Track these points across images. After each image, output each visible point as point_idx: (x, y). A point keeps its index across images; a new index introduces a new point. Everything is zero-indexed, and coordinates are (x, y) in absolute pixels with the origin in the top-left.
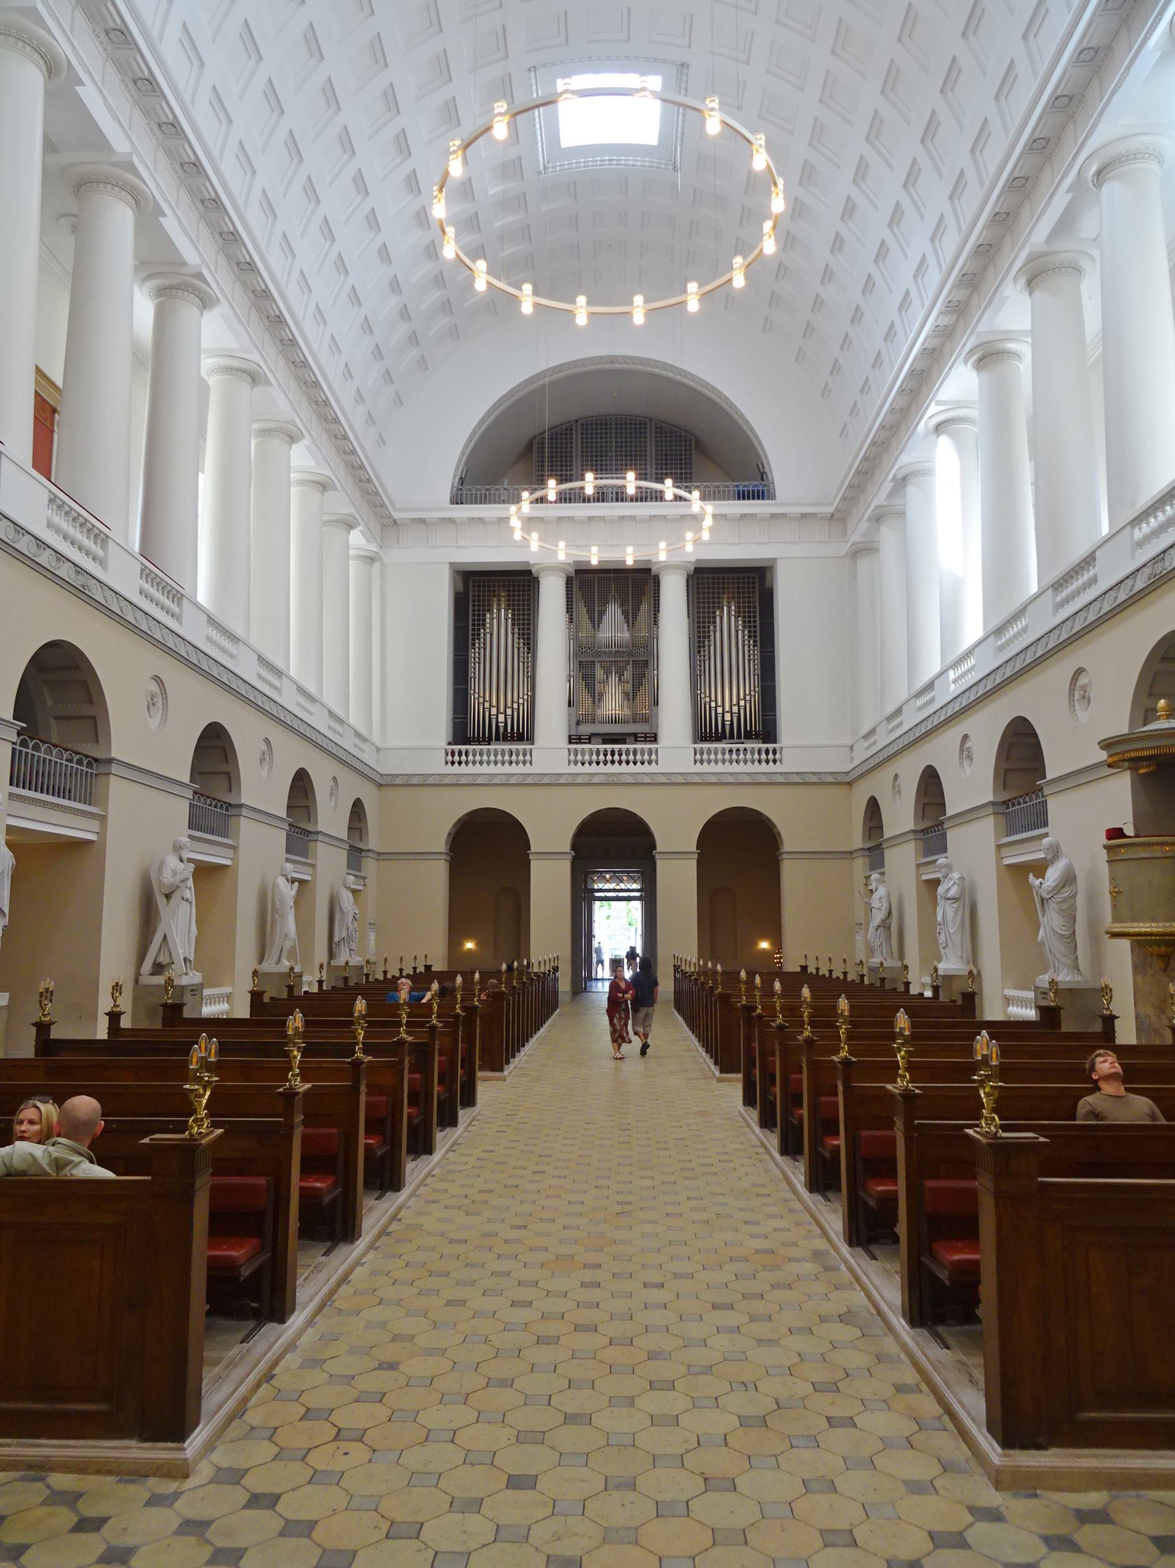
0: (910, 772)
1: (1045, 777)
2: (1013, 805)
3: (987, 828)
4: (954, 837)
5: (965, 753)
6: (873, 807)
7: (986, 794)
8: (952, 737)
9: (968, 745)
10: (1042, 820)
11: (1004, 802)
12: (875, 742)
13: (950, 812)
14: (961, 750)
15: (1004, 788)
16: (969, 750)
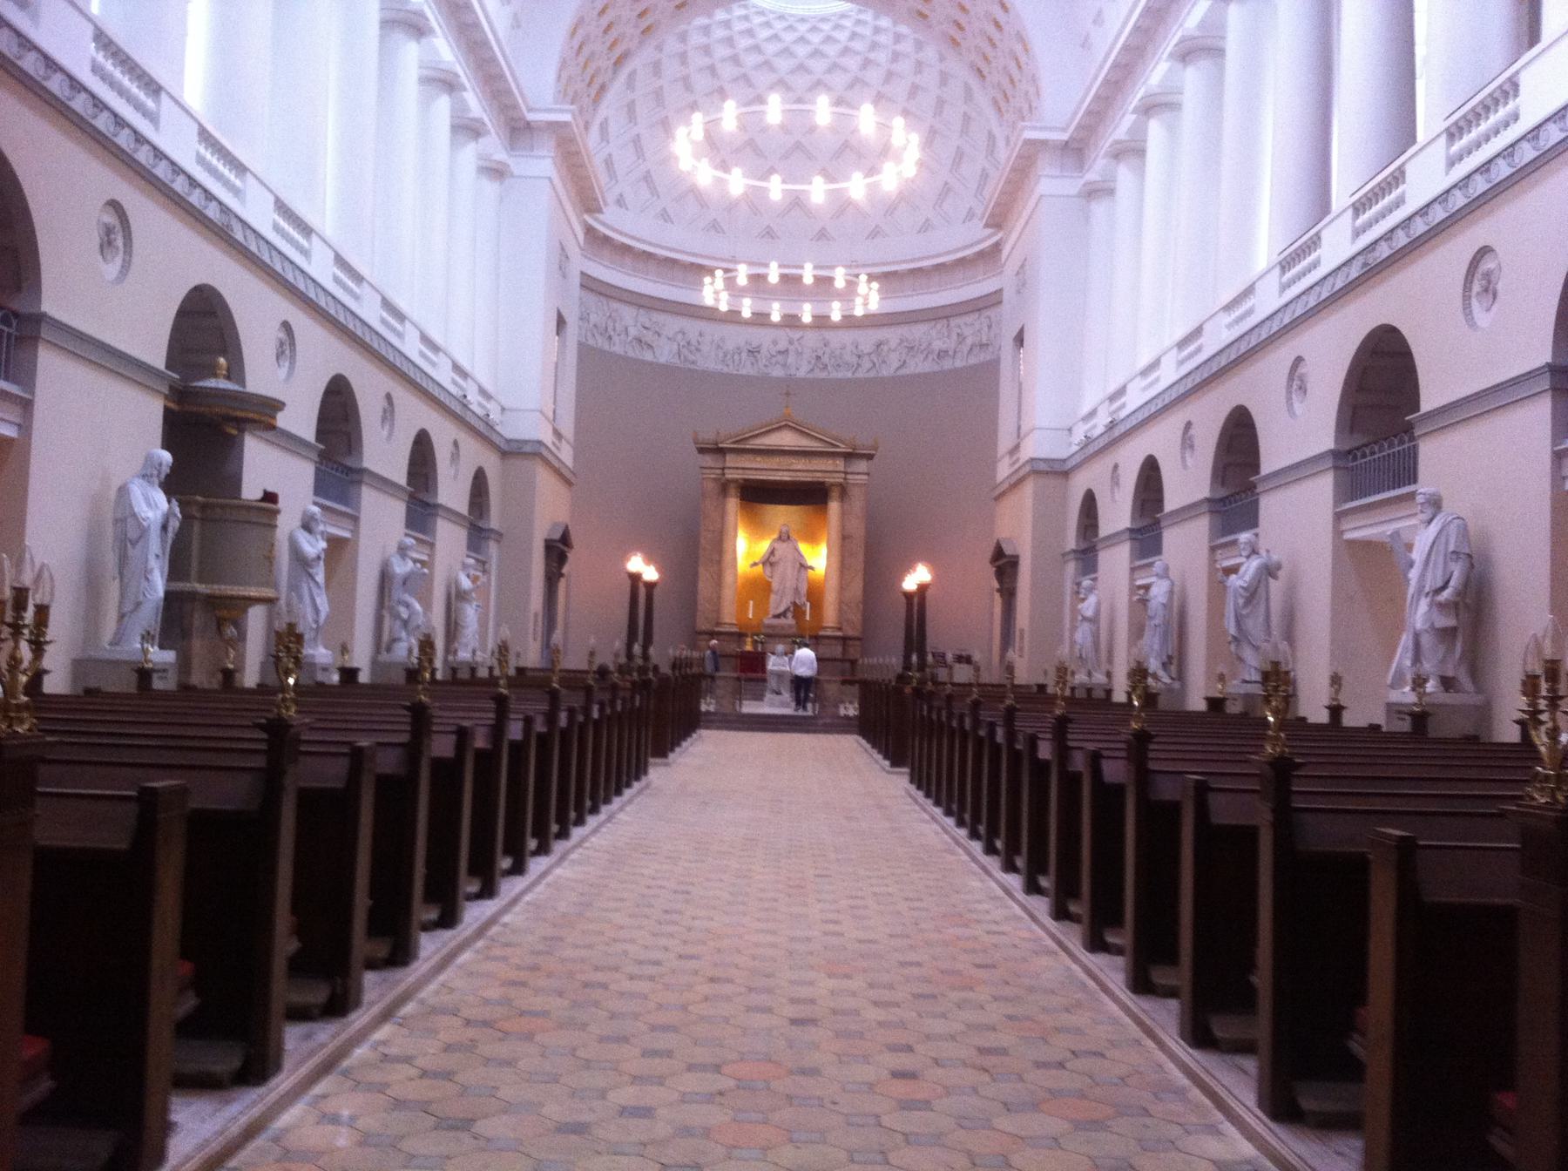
0: (1209, 416)
1: (1416, 408)
2: (1364, 456)
3: (1322, 489)
4: (1271, 506)
5: (1296, 383)
6: (1150, 474)
7: (1323, 438)
8: (1279, 360)
9: (1301, 370)
10: (1407, 471)
11: (1349, 452)
12: (1157, 380)
13: (1266, 468)
14: (1289, 386)
15: (1352, 431)
16: (1301, 379)
